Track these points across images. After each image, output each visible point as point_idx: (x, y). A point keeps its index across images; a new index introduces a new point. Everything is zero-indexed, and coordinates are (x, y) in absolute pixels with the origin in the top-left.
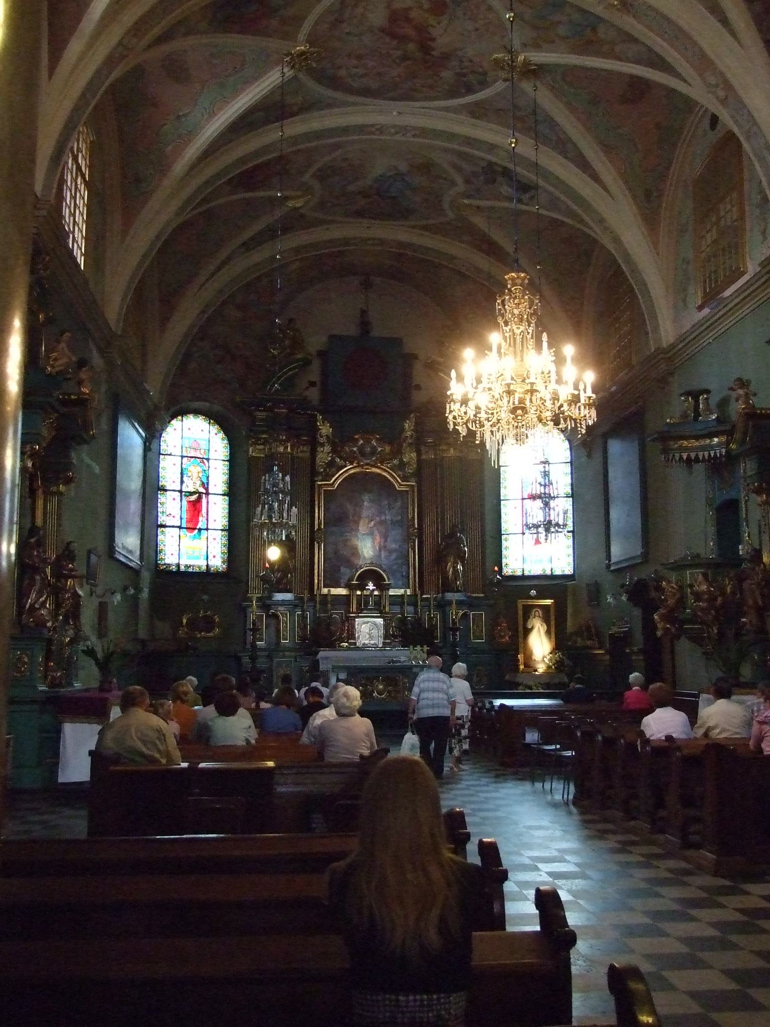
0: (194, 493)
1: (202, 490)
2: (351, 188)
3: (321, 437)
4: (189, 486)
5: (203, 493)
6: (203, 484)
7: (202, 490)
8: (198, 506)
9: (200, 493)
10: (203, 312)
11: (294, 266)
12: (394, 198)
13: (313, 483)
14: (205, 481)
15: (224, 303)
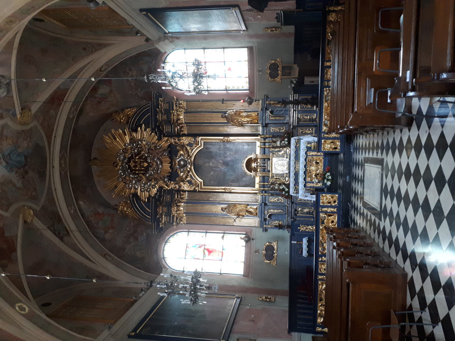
0: (204, 252)
1: (203, 247)
2: (19, 185)
3: (176, 187)
4: (201, 255)
5: (204, 247)
6: (200, 247)
7: (203, 247)
8: (211, 250)
9: (204, 249)
10: (104, 256)
11: (81, 203)
12: (26, 157)
13: (199, 192)
14: (198, 246)
15: (103, 241)
